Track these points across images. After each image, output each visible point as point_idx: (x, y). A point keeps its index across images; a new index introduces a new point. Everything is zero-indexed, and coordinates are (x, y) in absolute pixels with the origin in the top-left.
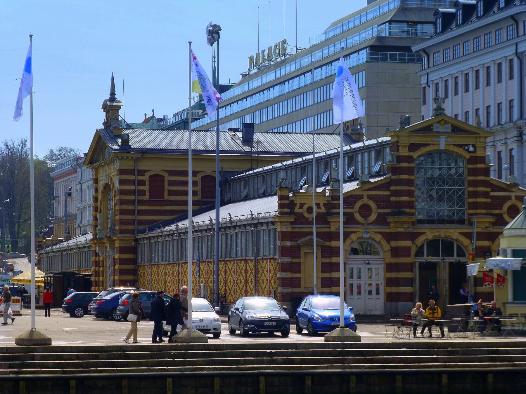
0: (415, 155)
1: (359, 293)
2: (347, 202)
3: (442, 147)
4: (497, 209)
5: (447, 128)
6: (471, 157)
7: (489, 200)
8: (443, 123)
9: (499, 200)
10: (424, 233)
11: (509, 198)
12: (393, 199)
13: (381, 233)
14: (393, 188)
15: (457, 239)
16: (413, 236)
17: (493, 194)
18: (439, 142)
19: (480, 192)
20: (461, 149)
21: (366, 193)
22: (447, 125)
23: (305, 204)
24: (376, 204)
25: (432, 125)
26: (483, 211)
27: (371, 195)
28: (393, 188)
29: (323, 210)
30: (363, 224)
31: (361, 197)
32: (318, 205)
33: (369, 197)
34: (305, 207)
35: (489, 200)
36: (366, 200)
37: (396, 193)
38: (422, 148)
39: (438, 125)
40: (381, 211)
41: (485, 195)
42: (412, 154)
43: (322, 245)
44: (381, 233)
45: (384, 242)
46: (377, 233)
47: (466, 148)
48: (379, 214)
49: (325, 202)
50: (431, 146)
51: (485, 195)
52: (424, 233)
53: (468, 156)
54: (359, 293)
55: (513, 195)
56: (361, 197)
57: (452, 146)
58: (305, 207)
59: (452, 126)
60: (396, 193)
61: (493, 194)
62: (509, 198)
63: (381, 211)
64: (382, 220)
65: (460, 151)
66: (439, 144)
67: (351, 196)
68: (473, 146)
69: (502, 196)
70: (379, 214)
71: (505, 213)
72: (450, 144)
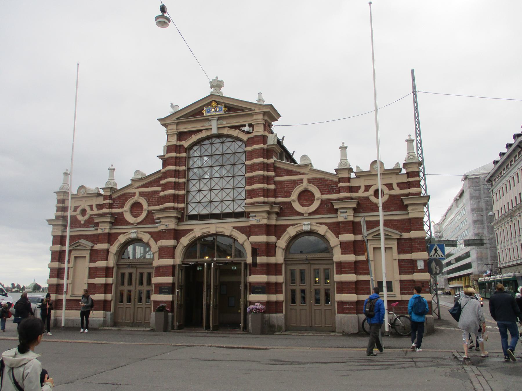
0: (186, 144)
1: (129, 301)
2: (119, 202)
3: (214, 131)
4: (286, 197)
5: (220, 110)
6: (249, 138)
7: (272, 187)
8: (214, 104)
9: (287, 186)
10: (192, 230)
11: (301, 181)
12: (162, 194)
13: (150, 233)
14: (162, 182)
15: (231, 235)
16: (177, 235)
17: (278, 179)
18: (211, 126)
19: (256, 176)
20: (238, 131)
21: (137, 191)
22: (220, 106)
23: (79, 206)
24: (148, 202)
25: (202, 108)
26: (261, 199)
27: (143, 192)
28: (162, 182)
29: (96, 211)
30: (132, 224)
31: (134, 194)
32: (91, 206)
33: (142, 194)
34: (79, 209)
35: (272, 187)
36: (136, 198)
37: (165, 187)
38: (193, 136)
39: (209, 108)
40: (152, 208)
41: (266, 180)
42: (182, 143)
43: (90, 248)
44: (150, 233)
45: (152, 242)
46: (146, 232)
47: (243, 129)
48: (149, 212)
49: (98, 203)
50: (204, 131)
51: (266, 180)
52: (192, 230)
53: (245, 137)
54: (129, 301)
55: (305, 178)
56: (134, 194)
57: (227, 128)
58: (79, 209)
59: (226, 107)
60: (165, 187)
61: (278, 179)
62: (301, 181)
63: (152, 208)
64: (150, 219)
65: (235, 133)
66: (211, 129)
67: (124, 195)
68: (251, 125)
69: (291, 181)
70: (149, 212)
71: (294, 201)
72: (225, 127)
